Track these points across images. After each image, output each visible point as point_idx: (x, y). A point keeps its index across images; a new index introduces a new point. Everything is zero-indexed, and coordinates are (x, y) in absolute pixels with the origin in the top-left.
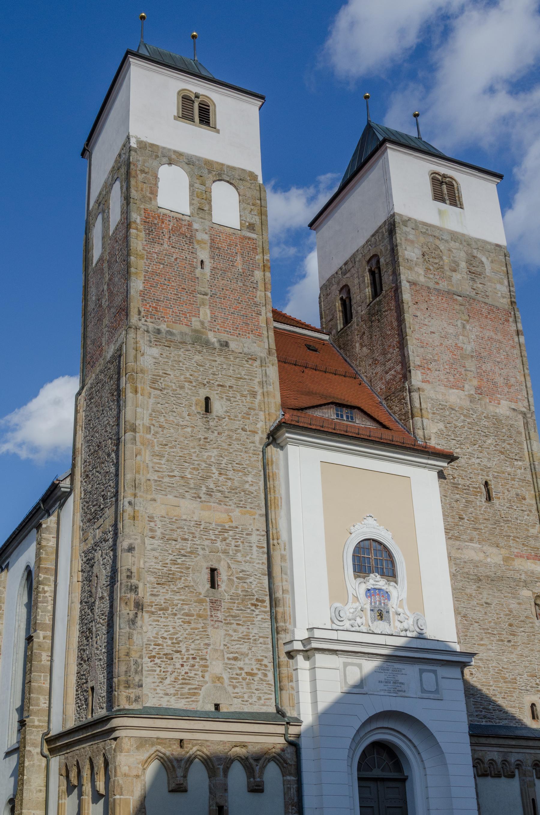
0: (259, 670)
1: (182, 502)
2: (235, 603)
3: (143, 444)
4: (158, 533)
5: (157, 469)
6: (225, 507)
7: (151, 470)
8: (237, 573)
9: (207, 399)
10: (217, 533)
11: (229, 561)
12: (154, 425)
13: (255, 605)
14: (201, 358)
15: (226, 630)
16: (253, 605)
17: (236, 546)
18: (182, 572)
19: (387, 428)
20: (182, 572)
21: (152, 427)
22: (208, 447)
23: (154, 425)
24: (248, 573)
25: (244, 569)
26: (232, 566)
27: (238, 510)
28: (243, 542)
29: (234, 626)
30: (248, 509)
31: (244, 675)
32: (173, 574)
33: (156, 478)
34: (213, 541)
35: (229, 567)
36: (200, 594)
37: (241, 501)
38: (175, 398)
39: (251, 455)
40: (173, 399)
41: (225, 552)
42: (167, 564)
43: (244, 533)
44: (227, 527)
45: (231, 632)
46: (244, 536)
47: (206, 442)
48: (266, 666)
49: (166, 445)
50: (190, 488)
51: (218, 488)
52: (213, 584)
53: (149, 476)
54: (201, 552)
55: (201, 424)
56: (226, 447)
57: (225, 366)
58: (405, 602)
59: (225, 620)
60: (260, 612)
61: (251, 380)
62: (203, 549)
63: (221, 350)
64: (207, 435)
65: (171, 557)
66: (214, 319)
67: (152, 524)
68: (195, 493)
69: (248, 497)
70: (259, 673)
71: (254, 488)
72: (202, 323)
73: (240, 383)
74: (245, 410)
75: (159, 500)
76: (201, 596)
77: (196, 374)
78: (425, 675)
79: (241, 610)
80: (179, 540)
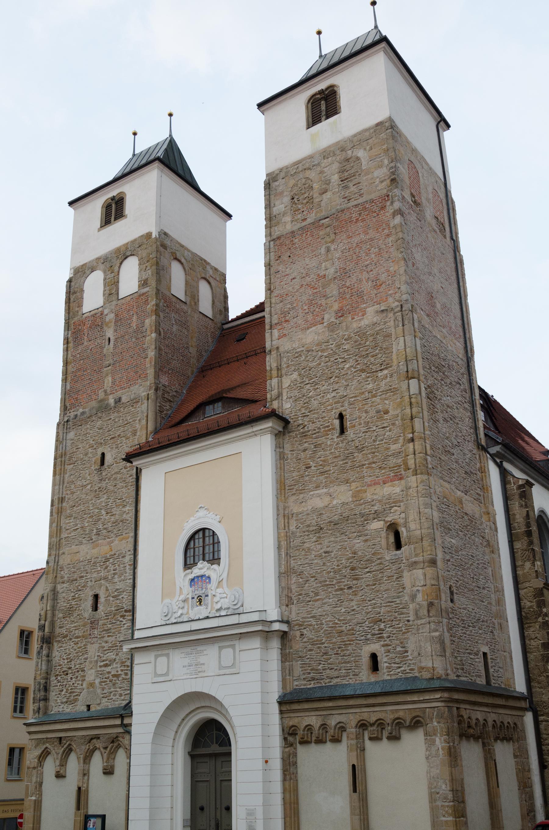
2: (108, 619)
4: (66, 579)
5: (68, 528)
6: (108, 540)
8: (113, 593)
9: (103, 455)
10: (102, 564)
11: (108, 585)
12: (67, 494)
14: (101, 422)
15: (100, 643)
16: (121, 616)
17: (114, 570)
19: (256, 401)
20: (77, 604)
23: (67, 494)
24: (121, 590)
25: (118, 587)
26: (109, 588)
27: (117, 539)
28: (119, 565)
29: (106, 639)
30: (124, 535)
31: (111, 677)
33: (66, 536)
34: (98, 572)
35: (107, 590)
37: (119, 530)
38: (82, 466)
41: (105, 578)
42: (69, 600)
43: (120, 557)
45: (103, 644)
46: (120, 560)
47: (99, 491)
49: (74, 506)
50: (86, 535)
51: (105, 526)
52: (95, 608)
54: (90, 584)
57: (116, 420)
59: (100, 635)
60: (126, 621)
61: (133, 421)
62: (91, 581)
64: (100, 485)
65: (73, 594)
68: (89, 537)
69: (125, 524)
70: (123, 673)
71: (129, 515)
75: (66, 552)
77: (97, 438)
78: (224, 651)
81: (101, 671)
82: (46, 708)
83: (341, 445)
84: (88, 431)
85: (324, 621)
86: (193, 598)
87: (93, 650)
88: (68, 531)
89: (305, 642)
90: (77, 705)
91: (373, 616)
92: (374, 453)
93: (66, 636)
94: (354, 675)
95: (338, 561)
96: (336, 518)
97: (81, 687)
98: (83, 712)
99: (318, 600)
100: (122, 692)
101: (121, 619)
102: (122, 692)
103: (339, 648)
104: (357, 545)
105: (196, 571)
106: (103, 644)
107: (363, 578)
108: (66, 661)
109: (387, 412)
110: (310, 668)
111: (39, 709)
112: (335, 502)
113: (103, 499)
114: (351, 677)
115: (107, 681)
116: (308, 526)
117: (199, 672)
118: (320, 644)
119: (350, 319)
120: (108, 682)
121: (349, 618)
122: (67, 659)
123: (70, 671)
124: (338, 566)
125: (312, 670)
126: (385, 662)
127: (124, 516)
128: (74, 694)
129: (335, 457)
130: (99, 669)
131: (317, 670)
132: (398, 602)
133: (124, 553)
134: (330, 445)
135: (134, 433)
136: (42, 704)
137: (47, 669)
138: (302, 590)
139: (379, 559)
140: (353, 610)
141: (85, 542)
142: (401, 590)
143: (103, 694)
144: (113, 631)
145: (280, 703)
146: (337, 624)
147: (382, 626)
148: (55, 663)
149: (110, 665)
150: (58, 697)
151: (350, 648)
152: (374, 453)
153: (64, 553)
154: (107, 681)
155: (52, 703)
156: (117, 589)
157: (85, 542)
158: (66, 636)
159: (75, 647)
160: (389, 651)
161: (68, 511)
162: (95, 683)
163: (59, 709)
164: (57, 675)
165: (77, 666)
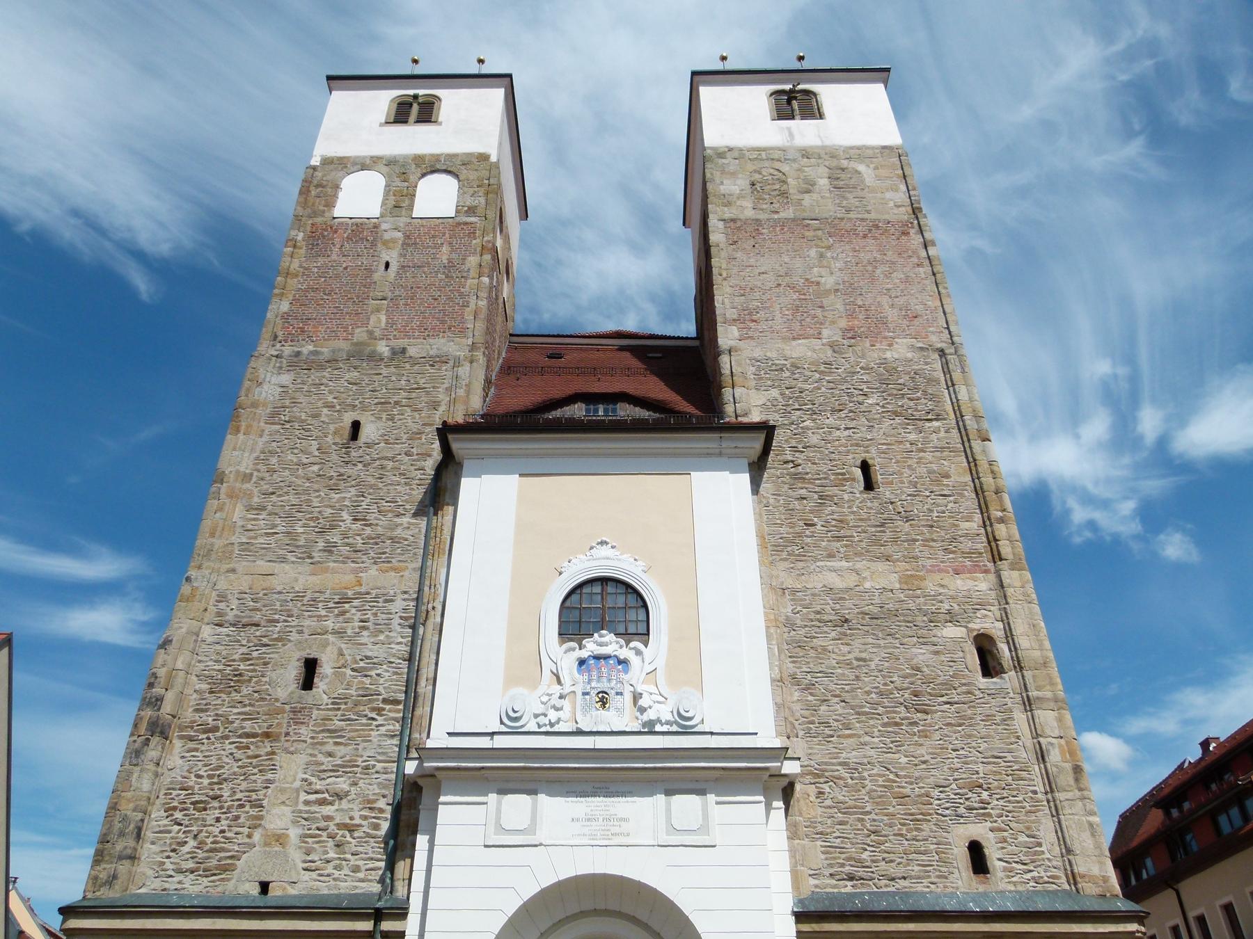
0: (365, 818)
1: (277, 568)
2: (339, 709)
3: (230, 496)
5: (250, 527)
7: (239, 530)
9: (356, 426)
10: (331, 605)
11: (343, 646)
12: (259, 471)
13: (379, 711)
16: (373, 709)
18: (255, 670)
21: (255, 474)
22: (342, 485)
25: (370, 654)
28: (375, 615)
31: (332, 828)
32: (240, 675)
35: (341, 654)
36: (277, 700)
39: (415, 487)
40: (297, 432)
41: (340, 633)
44: (350, 593)
45: (321, 758)
48: (381, 811)
50: (298, 547)
53: (234, 539)
54: (294, 636)
55: (337, 457)
56: (373, 481)
57: (393, 378)
58: (660, 674)
59: (312, 738)
63: (392, 359)
64: (342, 470)
65: (244, 650)
66: (391, 323)
67: (222, 605)
72: (371, 333)
73: (414, 395)
74: (415, 428)
76: (278, 704)
79: (349, 720)
80: (263, 623)
81: (307, 812)
82: (131, 877)
83: (869, 504)
84: (324, 381)
85: (865, 774)
86: (585, 694)
87: (292, 768)
88: (252, 534)
89: (830, 807)
90: (228, 880)
91: (964, 776)
92: (932, 526)
93: (216, 729)
94: (939, 877)
95: (884, 677)
96: (875, 610)
97: (247, 840)
98: (247, 896)
99: (850, 736)
100: (361, 863)
101: (373, 715)
102: (361, 863)
103: (904, 825)
104: (921, 657)
105: (591, 647)
106: (321, 758)
107: (936, 711)
108: (206, 782)
109: (947, 476)
110: (843, 856)
111: (115, 877)
112: (867, 585)
113: (348, 495)
114: (933, 880)
115: (320, 836)
116: (818, 613)
117: (616, 834)
118: (862, 813)
119: (868, 344)
120: (324, 838)
121: (917, 774)
122: (210, 777)
123: (216, 804)
124: (885, 684)
125: (848, 859)
126: (1000, 860)
127: (399, 531)
128: (222, 854)
129: (861, 520)
130: (302, 807)
131: (859, 861)
132: (1010, 758)
133: (392, 592)
134: (849, 501)
135: (435, 405)
136: (123, 868)
137: (150, 792)
138: (813, 715)
139: (964, 685)
140: (924, 762)
141: (294, 559)
142: (1014, 740)
143: (305, 862)
144: (348, 735)
145: (800, 917)
146: (895, 782)
147: (985, 795)
148: (172, 783)
149: (331, 804)
150: (168, 857)
151: (925, 826)
152: (932, 526)
153: (233, 571)
154: (320, 836)
155: (144, 868)
156: (367, 658)
157: (294, 559)
158: (216, 729)
159: (239, 754)
160: (1005, 841)
161: (256, 500)
162: (288, 836)
163: (167, 885)
164: (175, 808)
165: (239, 796)
